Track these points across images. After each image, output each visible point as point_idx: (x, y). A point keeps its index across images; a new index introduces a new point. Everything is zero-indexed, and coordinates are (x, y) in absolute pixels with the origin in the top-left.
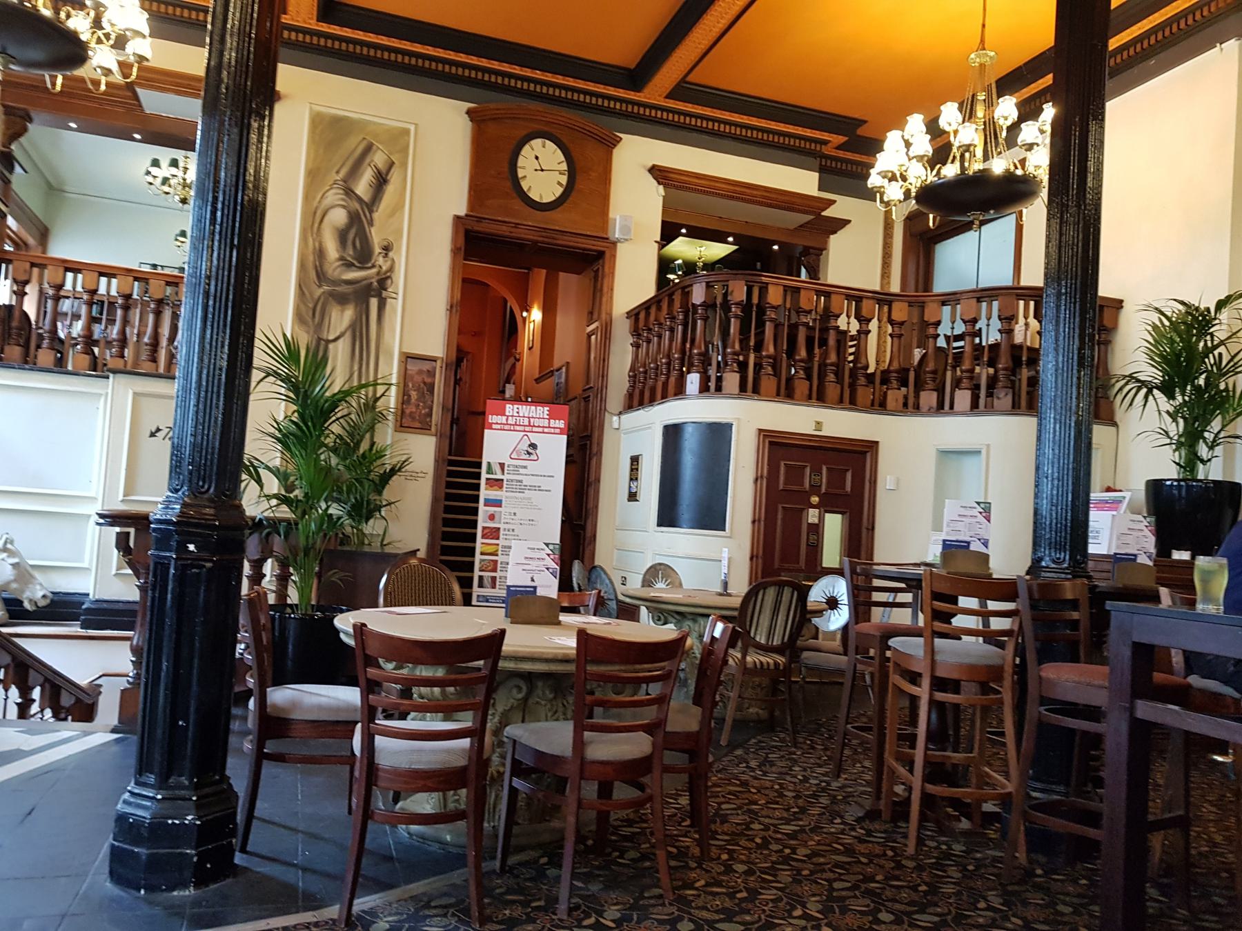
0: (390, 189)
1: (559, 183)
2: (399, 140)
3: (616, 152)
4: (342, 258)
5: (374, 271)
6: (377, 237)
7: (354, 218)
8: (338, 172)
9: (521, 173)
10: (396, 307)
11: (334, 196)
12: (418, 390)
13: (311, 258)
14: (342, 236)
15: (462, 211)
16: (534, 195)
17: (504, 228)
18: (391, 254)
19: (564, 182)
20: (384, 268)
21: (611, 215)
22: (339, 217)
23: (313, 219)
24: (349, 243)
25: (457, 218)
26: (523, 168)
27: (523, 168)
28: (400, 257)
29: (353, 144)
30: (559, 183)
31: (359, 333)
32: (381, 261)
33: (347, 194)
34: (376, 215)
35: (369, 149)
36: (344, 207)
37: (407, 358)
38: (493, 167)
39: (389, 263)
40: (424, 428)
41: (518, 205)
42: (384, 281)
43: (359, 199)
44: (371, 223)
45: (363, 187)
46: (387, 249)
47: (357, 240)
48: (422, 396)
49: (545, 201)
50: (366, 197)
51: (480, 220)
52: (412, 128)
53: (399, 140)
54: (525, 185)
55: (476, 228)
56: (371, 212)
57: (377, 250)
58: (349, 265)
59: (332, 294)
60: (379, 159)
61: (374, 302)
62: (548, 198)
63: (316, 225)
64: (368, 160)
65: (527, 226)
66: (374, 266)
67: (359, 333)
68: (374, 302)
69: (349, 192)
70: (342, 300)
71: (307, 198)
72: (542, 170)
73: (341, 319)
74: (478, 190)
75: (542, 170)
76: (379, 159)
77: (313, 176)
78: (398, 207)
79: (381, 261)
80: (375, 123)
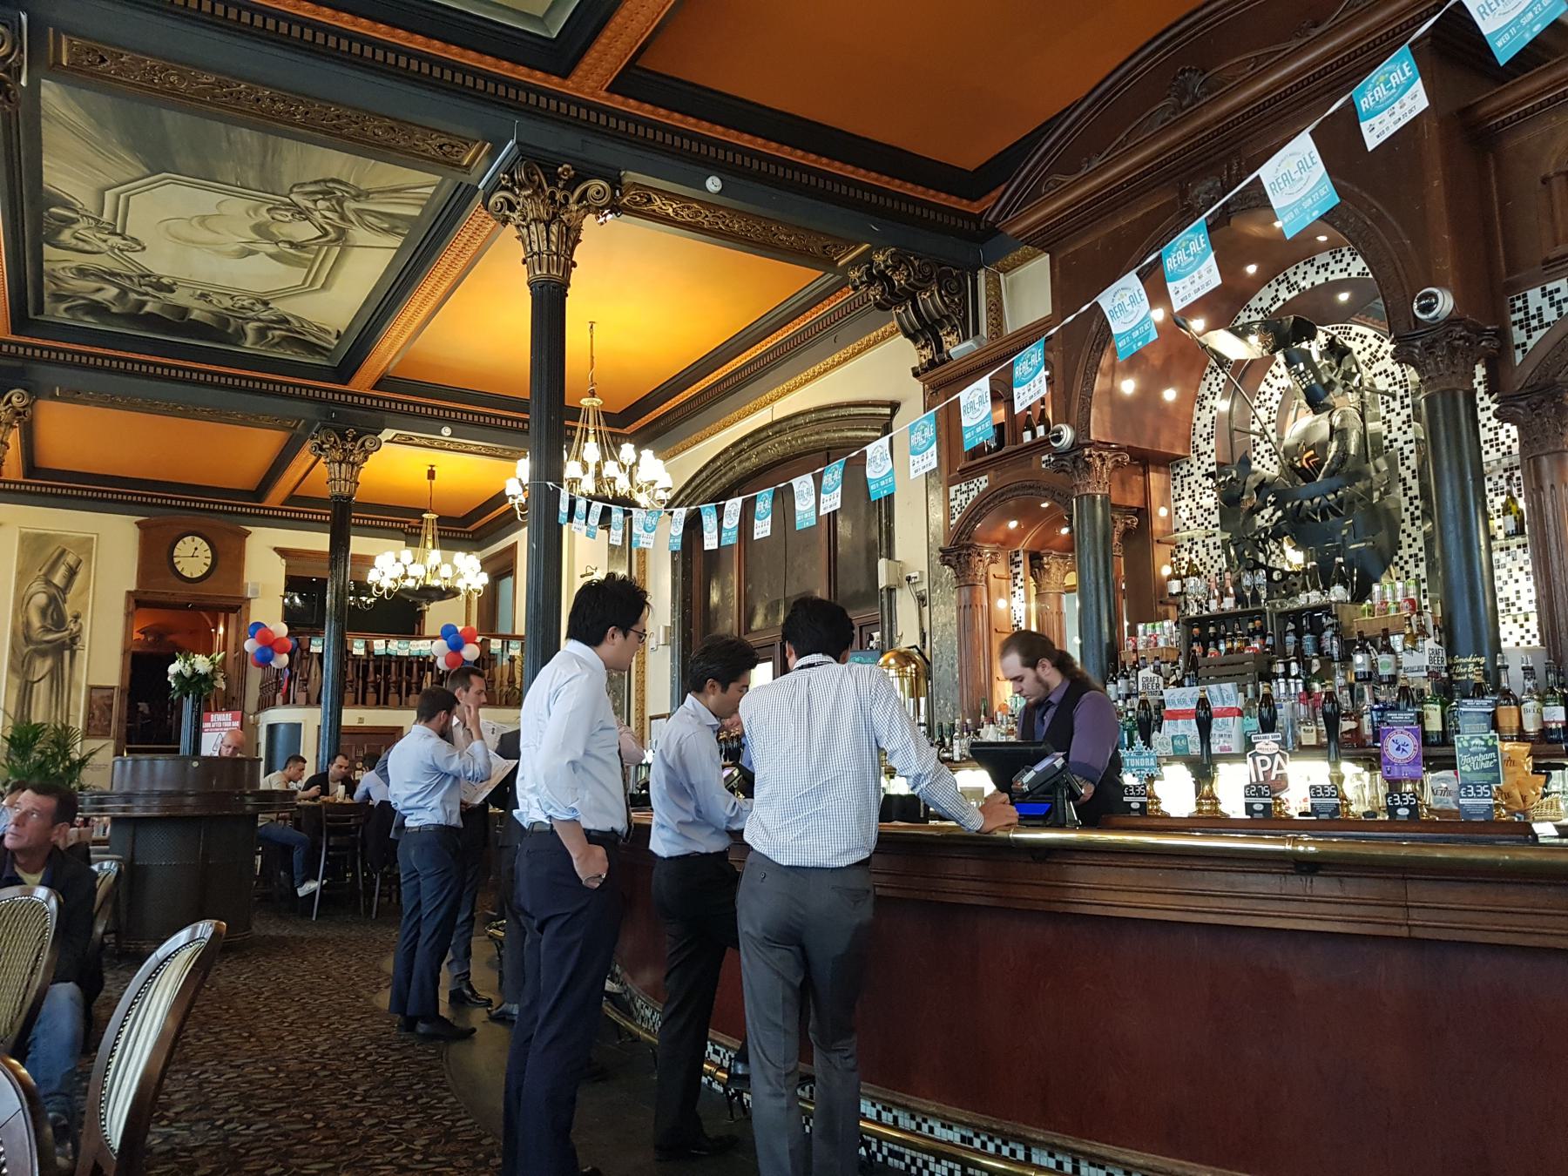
7: (52, 600)
10: (83, 656)
12: (100, 708)
14: (43, 612)
15: (133, 587)
25: (129, 593)
28: (86, 623)
31: (56, 675)
34: (68, 596)
35: (63, 553)
37: (91, 688)
38: (155, 554)
40: (105, 734)
41: (174, 580)
42: (74, 639)
43: (56, 587)
45: (58, 579)
46: (76, 617)
47: (54, 613)
48: (103, 713)
54: (179, 568)
58: (49, 631)
59: (35, 651)
60: (70, 559)
61: (67, 653)
65: (183, 593)
67: (56, 675)
68: (67, 653)
70: (44, 654)
72: (192, 557)
73: (43, 666)
74: (144, 573)
75: (192, 557)
76: (70, 559)
78: (85, 589)
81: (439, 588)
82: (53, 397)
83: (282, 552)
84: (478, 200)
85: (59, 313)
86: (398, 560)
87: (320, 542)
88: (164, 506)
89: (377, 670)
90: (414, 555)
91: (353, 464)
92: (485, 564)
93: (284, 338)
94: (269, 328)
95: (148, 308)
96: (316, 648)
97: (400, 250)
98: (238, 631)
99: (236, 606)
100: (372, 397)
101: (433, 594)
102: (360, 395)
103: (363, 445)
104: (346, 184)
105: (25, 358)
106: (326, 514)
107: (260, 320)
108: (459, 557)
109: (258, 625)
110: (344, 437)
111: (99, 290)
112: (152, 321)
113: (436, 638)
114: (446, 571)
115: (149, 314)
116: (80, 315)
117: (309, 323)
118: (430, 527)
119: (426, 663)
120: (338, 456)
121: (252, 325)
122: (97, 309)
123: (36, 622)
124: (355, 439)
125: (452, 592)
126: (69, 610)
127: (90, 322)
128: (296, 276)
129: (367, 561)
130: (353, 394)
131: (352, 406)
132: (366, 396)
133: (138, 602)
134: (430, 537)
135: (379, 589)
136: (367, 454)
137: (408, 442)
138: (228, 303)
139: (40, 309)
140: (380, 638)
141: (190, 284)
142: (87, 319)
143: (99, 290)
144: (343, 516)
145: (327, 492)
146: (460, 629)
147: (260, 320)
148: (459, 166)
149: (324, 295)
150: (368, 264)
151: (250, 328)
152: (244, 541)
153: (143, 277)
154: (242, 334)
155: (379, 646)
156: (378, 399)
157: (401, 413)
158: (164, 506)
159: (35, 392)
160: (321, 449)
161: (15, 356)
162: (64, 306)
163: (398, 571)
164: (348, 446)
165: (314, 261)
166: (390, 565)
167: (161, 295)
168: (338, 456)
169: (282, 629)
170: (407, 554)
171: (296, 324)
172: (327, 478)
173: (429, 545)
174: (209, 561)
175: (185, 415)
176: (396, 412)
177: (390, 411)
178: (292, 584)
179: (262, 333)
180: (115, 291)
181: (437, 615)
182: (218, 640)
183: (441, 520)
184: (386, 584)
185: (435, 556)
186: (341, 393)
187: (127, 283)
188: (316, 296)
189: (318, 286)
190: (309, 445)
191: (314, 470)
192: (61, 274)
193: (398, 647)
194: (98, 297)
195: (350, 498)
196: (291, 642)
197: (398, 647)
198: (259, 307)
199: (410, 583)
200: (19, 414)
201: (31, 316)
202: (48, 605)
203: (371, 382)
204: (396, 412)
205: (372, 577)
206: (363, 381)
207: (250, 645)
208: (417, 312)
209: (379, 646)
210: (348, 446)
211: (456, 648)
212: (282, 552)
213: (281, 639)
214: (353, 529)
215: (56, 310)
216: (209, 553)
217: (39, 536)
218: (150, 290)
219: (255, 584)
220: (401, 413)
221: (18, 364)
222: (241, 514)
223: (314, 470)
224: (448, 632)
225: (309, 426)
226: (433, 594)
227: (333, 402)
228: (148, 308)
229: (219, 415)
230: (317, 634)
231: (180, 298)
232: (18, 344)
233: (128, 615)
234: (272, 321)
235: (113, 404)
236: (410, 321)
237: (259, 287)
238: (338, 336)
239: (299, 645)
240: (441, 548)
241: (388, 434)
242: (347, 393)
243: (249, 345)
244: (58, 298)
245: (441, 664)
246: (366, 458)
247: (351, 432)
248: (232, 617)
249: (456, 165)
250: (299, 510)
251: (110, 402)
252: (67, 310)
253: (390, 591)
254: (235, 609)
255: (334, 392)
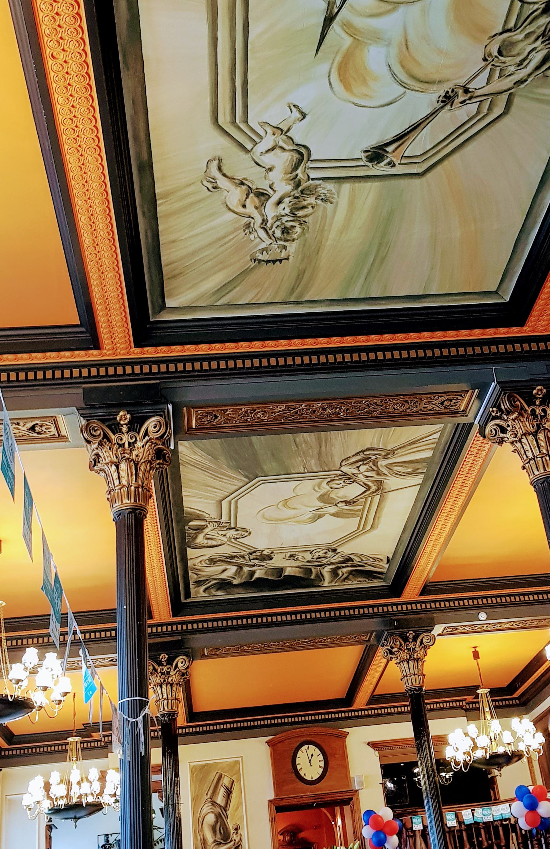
0: (234, 795)
1: (320, 766)
2: (235, 767)
3: (347, 739)
4: (215, 841)
5: (232, 843)
6: (231, 825)
7: (218, 817)
8: (207, 794)
9: (299, 767)
11: (207, 808)
13: (200, 845)
15: (272, 796)
16: (308, 778)
17: (295, 800)
18: (239, 832)
19: (323, 765)
20: (237, 841)
21: (352, 776)
22: (211, 819)
23: (199, 823)
24: (218, 832)
25: (270, 801)
26: (300, 764)
27: (300, 764)
28: (243, 831)
29: (212, 777)
30: (320, 766)
32: (235, 837)
33: (213, 805)
34: (228, 812)
35: (221, 776)
36: (212, 812)
38: (284, 766)
39: (239, 837)
41: (301, 785)
43: (219, 805)
44: (227, 817)
45: (220, 799)
46: (237, 829)
49: (314, 779)
50: (223, 804)
51: (282, 799)
52: (240, 759)
53: (235, 767)
55: (281, 804)
56: (226, 811)
57: (232, 831)
60: (226, 781)
62: (316, 777)
63: (200, 827)
64: (221, 783)
65: (307, 794)
66: (231, 841)
69: (214, 803)
71: (193, 813)
72: (310, 763)
74: (279, 783)
75: (310, 763)
76: (226, 781)
77: (195, 800)
79: (235, 837)
80: (221, 763)
81: (506, 753)
82: (203, 657)
83: (374, 745)
84: (476, 429)
85: (199, 594)
86: (466, 734)
87: (404, 730)
88: (286, 722)
89: (470, 838)
90: (478, 728)
91: (417, 660)
92: (537, 722)
93: (351, 573)
94: (339, 568)
95: (256, 576)
96: (418, 826)
97: (422, 485)
98: (354, 821)
99: (346, 800)
100: (421, 602)
101: (501, 760)
102: (411, 603)
103: (422, 642)
104: (377, 449)
105: (182, 632)
106: (406, 706)
107: (332, 564)
108: (515, 721)
109: (369, 813)
110: (406, 640)
111: (224, 570)
112: (261, 584)
113: (513, 800)
114: (507, 737)
115: (259, 579)
116: (213, 591)
117: (366, 556)
118: (486, 704)
119: (508, 826)
120: (404, 655)
121: (328, 568)
122: (224, 585)
123: (210, 838)
124: (415, 639)
125: (517, 756)
126: (231, 826)
127: (221, 595)
128: (352, 524)
129: (442, 740)
130: (406, 604)
131: (408, 613)
132: (416, 603)
133: (279, 807)
134: (487, 709)
135: (457, 764)
136: (426, 648)
137: (454, 632)
138: (308, 557)
139: (188, 595)
140: (466, 808)
141: (282, 549)
142: (219, 593)
143: (224, 570)
144: (418, 705)
145: (403, 687)
146: (531, 788)
147: (332, 564)
148: (457, 413)
149: (374, 532)
150: (401, 500)
151: (326, 571)
152: (344, 742)
153: (251, 554)
154: (320, 577)
155: (467, 815)
156: (425, 602)
157: (446, 609)
158: (286, 722)
159: (192, 656)
160: (392, 653)
161: (177, 633)
162: (203, 588)
163: (467, 745)
164: (411, 646)
165: (364, 508)
166: (461, 740)
167: (264, 563)
168: (404, 655)
169: (387, 814)
170: (472, 728)
171: (357, 559)
172: (400, 675)
173: (488, 716)
174: (322, 764)
175: (292, 648)
176: (441, 610)
177: (436, 610)
178: (388, 771)
179: (334, 573)
180: (232, 570)
181: (508, 780)
182: (339, 832)
183: (494, 692)
184: (461, 758)
185: (495, 725)
186: (397, 604)
187: (241, 561)
188: (368, 535)
189: (368, 527)
190: (381, 651)
191: (389, 673)
192: (199, 566)
193: (483, 814)
194: (224, 576)
195: (421, 689)
196: (397, 823)
197: (483, 814)
198: (330, 554)
199: (479, 754)
200: (183, 675)
201: (183, 601)
202: (216, 822)
203: (418, 590)
204: (441, 610)
205: (449, 753)
206: (412, 591)
207: (367, 832)
208: (443, 527)
209: (467, 815)
210: (411, 646)
211: (532, 807)
212: (374, 745)
213: (388, 822)
214: (428, 714)
215: (197, 592)
216: (321, 757)
217: (204, 766)
218: (256, 562)
219: (359, 777)
220: (446, 609)
221: (179, 638)
222: (342, 719)
223: (389, 673)
224: (522, 793)
225: (379, 638)
226: (501, 760)
227: (393, 613)
228: (256, 576)
229: (315, 643)
230: (415, 813)
231: (277, 562)
232: (176, 624)
233: (273, 820)
234: (341, 562)
235: (243, 653)
236: (439, 537)
237: (328, 539)
238: (388, 561)
239: (404, 825)
240: (500, 716)
241: (438, 629)
242: (401, 604)
243: (328, 584)
244: (199, 583)
245: (523, 824)
246: (426, 653)
247: (411, 634)
248: (347, 808)
249: (455, 413)
250: (382, 706)
251: (240, 650)
252: (205, 591)
253: (466, 764)
254: (347, 801)
255: (392, 605)
